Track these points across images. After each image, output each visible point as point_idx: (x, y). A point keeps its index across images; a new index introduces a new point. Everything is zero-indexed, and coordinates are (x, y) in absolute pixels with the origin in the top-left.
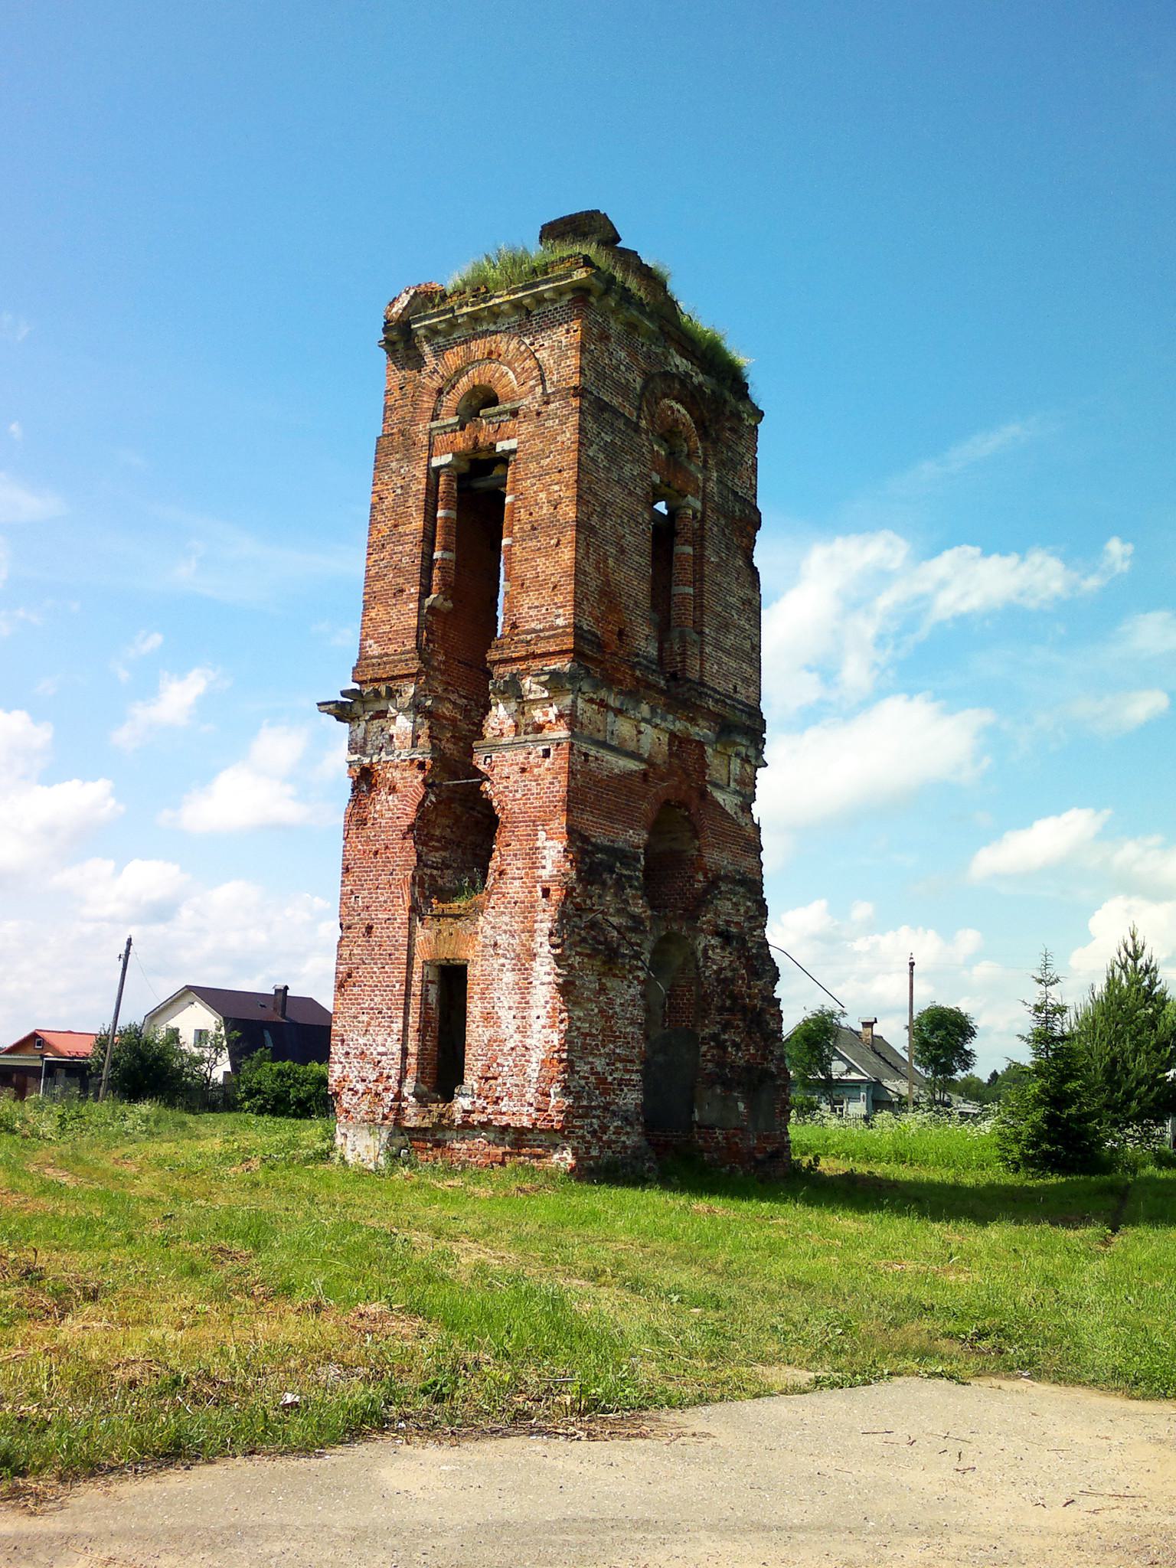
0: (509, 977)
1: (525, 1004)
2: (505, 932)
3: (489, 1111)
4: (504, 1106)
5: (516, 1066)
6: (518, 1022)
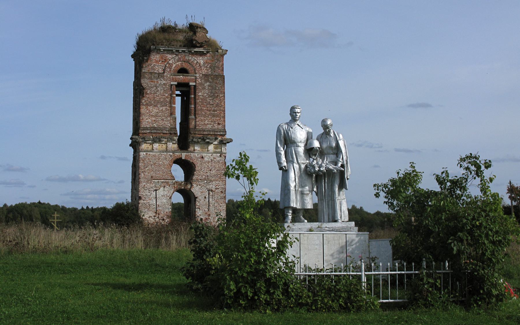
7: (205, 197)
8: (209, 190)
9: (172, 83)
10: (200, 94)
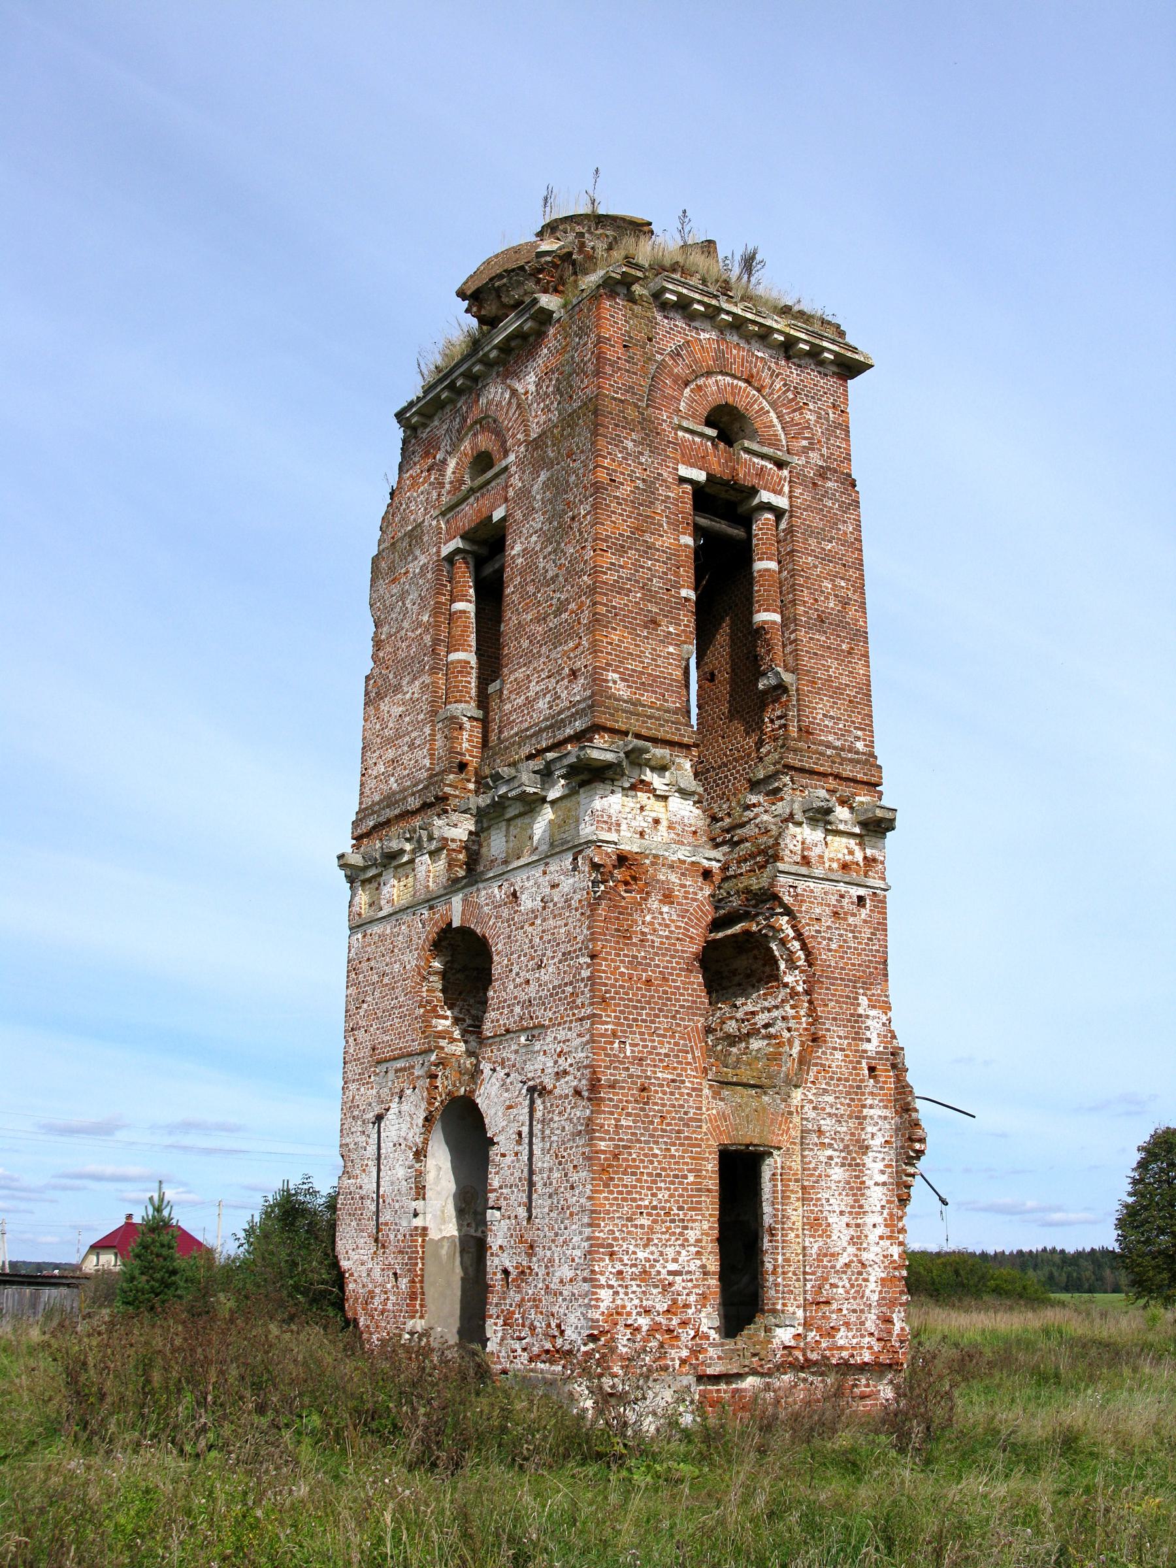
0: (838, 1173)
1: (858, 1209)
2: (830, 1115)
3: (824, 1345)
4: (842, 1338)
5: (852, 1286)
6: (852, 1231)
7: (520, 1134)
8: (532, 1090)
9: (446, 550)
10: (518, 548)
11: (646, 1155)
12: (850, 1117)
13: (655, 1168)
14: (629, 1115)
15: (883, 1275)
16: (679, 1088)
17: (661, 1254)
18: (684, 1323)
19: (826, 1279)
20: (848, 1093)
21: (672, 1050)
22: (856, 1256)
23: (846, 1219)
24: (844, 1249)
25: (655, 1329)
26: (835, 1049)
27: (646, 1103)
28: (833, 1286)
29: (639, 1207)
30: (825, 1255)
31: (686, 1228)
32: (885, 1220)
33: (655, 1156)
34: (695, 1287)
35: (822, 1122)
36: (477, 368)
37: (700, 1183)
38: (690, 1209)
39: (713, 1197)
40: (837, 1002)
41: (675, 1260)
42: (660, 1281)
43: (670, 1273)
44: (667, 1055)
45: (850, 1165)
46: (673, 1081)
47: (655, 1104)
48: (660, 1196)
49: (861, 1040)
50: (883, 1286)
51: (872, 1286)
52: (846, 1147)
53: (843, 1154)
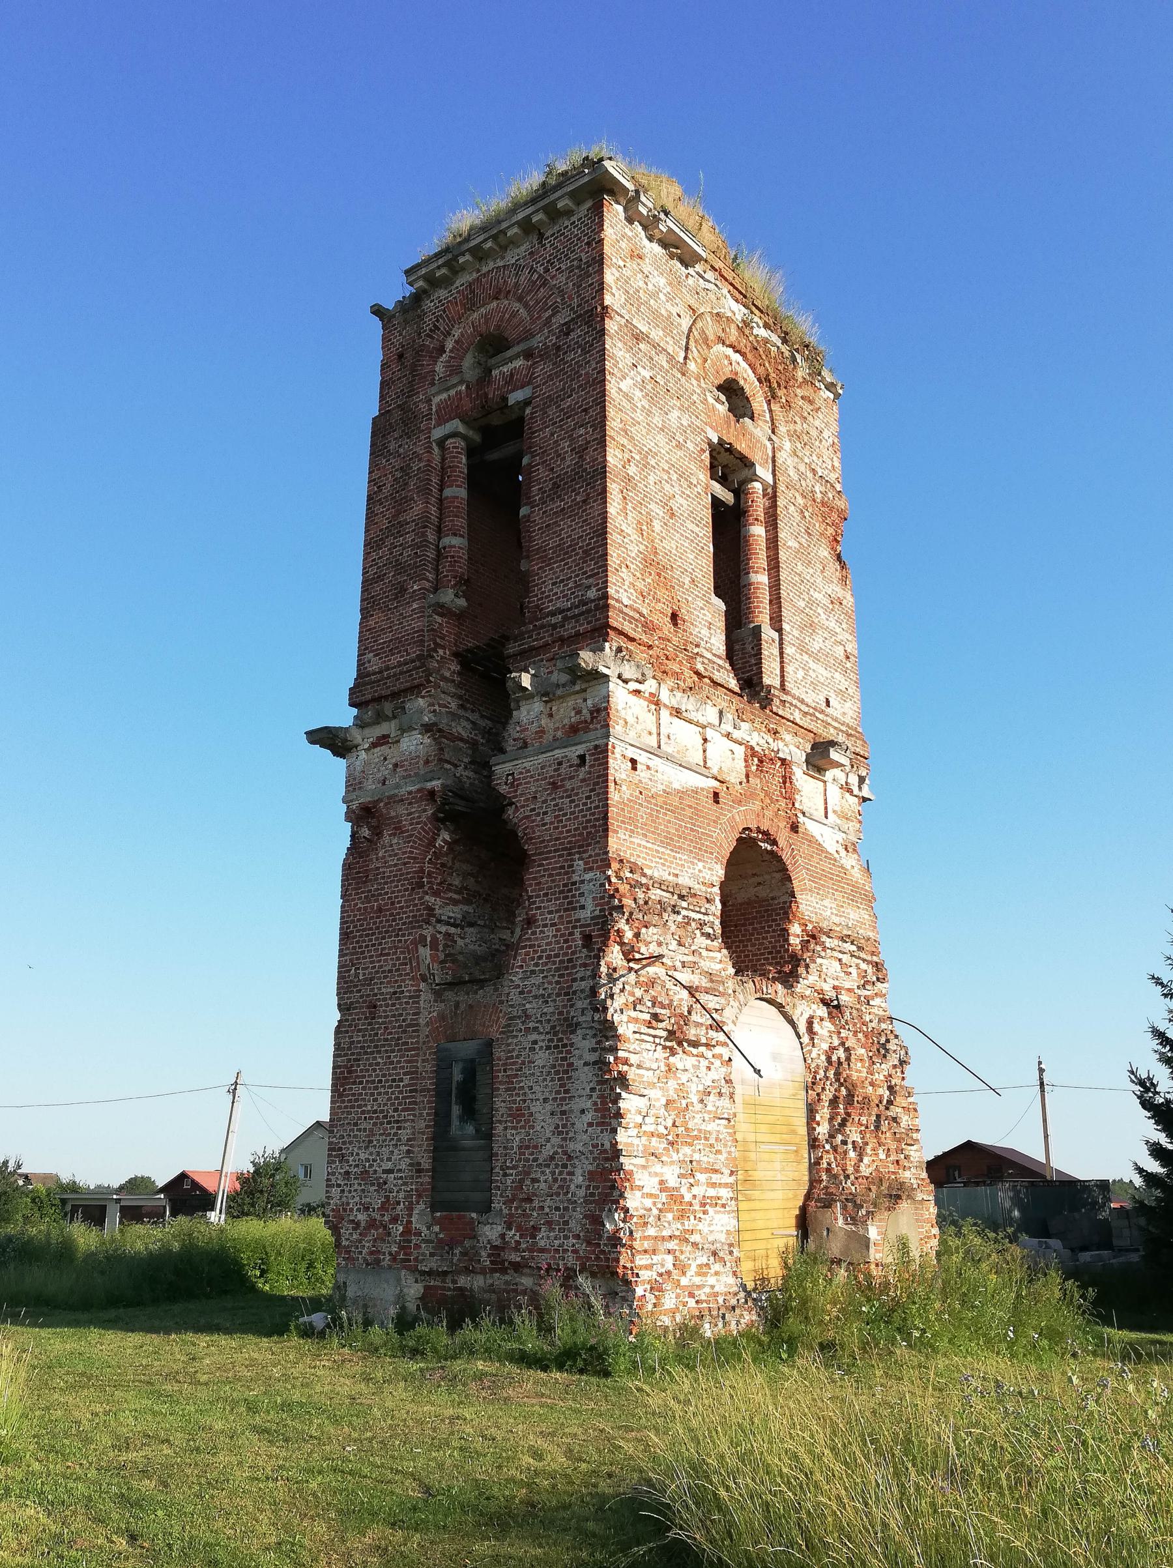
0: (542, 1058)
1: (564, 1093)
2: (536, 997)
3: (524, 1246)
4: (542, 1239)
5: (555, 1180)
6: (556, 1119)
11: (370, 1065)
12: (558, 995)
13: (377, 1076)
14: (359, 1031)
15: (590, 1168)
16: (399, 998)
17: (378, 1154)
18: (395, 1220)
19: (529, 1173)
20: (557, 970)
21: (394, 965)
22: (562, 1146)
23: (548, 1107)
24: (548, 1140)
25: (372, 1224)
26: (545, 926)
27: (374, 1018)
28: (534, 1181)
29: (363, 1112)
30: (528, 1147)
31: (399, 1128)
32: (595, 1104)
33: (378, 1064)
34: (405, 1184)
35: (528, 1006)
36: (489, 244)
37: (416, 1084)
38: (404, 1110)
39: (431, 1096)
40: (550, 875)
41: (389, 1159)
42: (377, 1179)
43: (385, 1172)
44: (390, 971)
45: (556, 1047)
46: (395, 993)
47: (380, 1017)
48: (380, 1101)
49: (574, 909)
50: (590, 1180)
51: (579, 1179)
52: (553, 1027)
53: (548, 1037)
